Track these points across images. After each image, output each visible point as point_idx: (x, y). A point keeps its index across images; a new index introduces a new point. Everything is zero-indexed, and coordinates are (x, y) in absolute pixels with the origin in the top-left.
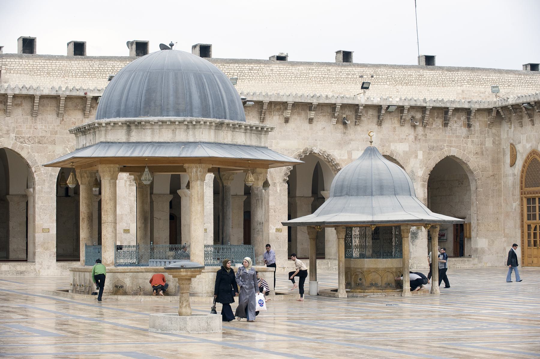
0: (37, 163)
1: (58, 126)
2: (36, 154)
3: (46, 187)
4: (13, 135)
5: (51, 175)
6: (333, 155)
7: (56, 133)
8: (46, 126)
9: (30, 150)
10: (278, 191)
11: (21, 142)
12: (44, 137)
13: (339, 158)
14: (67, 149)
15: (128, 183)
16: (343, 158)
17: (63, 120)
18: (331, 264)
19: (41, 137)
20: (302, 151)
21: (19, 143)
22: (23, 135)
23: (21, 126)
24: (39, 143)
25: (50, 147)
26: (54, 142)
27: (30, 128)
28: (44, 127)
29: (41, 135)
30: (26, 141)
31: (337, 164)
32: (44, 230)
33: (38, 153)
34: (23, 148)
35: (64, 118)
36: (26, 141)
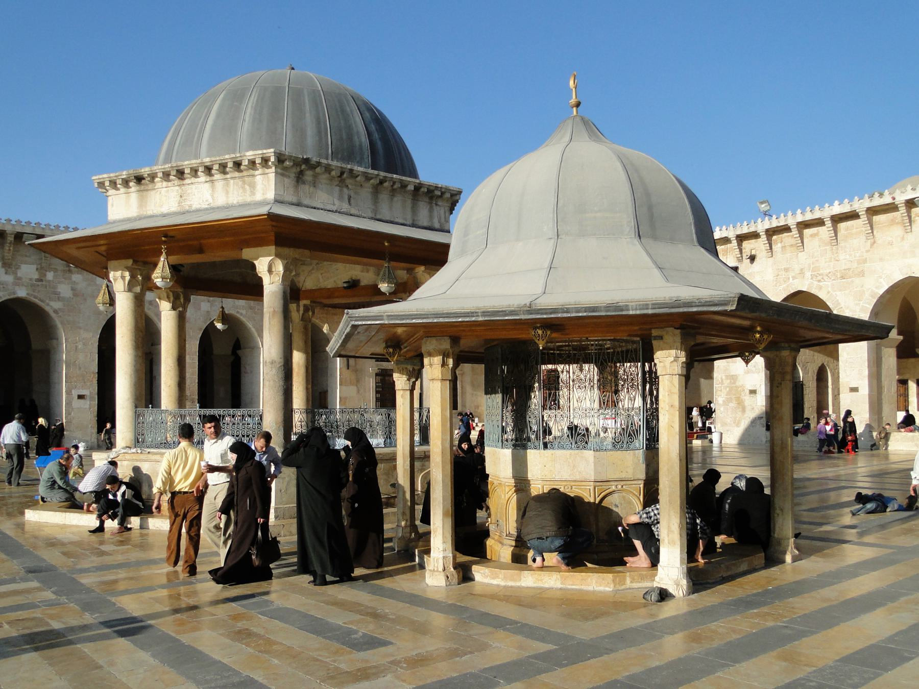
0: (839, 304)
1: (867, 251)
2: (838, 293)
4: (808, 274)
7: (865, 261)
8: (850, 255)
12: (849, 269)
21: (816, 283)
24: (843, 278)
25: (857, 281)
26: (862, 274)
27: (830, 261)
28: (848, 257)
30: (825, 278)
32: (854, 390)
34: (820, 288)
35: (877, 239)
36: (825, 278)
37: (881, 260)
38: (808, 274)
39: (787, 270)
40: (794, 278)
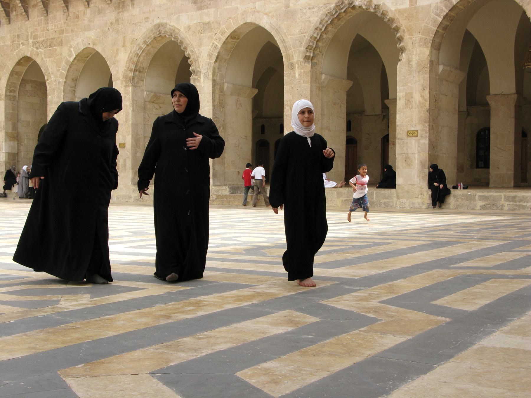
0: (48, 69)
2: (48, 60)
3: (56, 97)
4: (31, 41)
5: (59, 82)
6: (384, 4)
8: (55, 26)
9: (43, 56)
10: (297, 76)
11: (37, 48)
12: (54, 38)
13: (393, 9)
14: (72, 49)
15: (124, 83)
16: (401, 7)
17: (69, 15)
18: (377, 196)
19: (52, 39)
20: (333, 6)
22: (39, 40)
23: (36, 29)
24: (50, 46)
25: (58, 49)
26: (61, 44)
27: (43, 31)
28: (53, 28)
29: (52, 36)
30: (41, 45)
31: (392, 20)
33: (49, 58)
36: (41, 45)
37: (72, 31)
38: (31, 41)
39: (18, 36)
40: (23, 44)
